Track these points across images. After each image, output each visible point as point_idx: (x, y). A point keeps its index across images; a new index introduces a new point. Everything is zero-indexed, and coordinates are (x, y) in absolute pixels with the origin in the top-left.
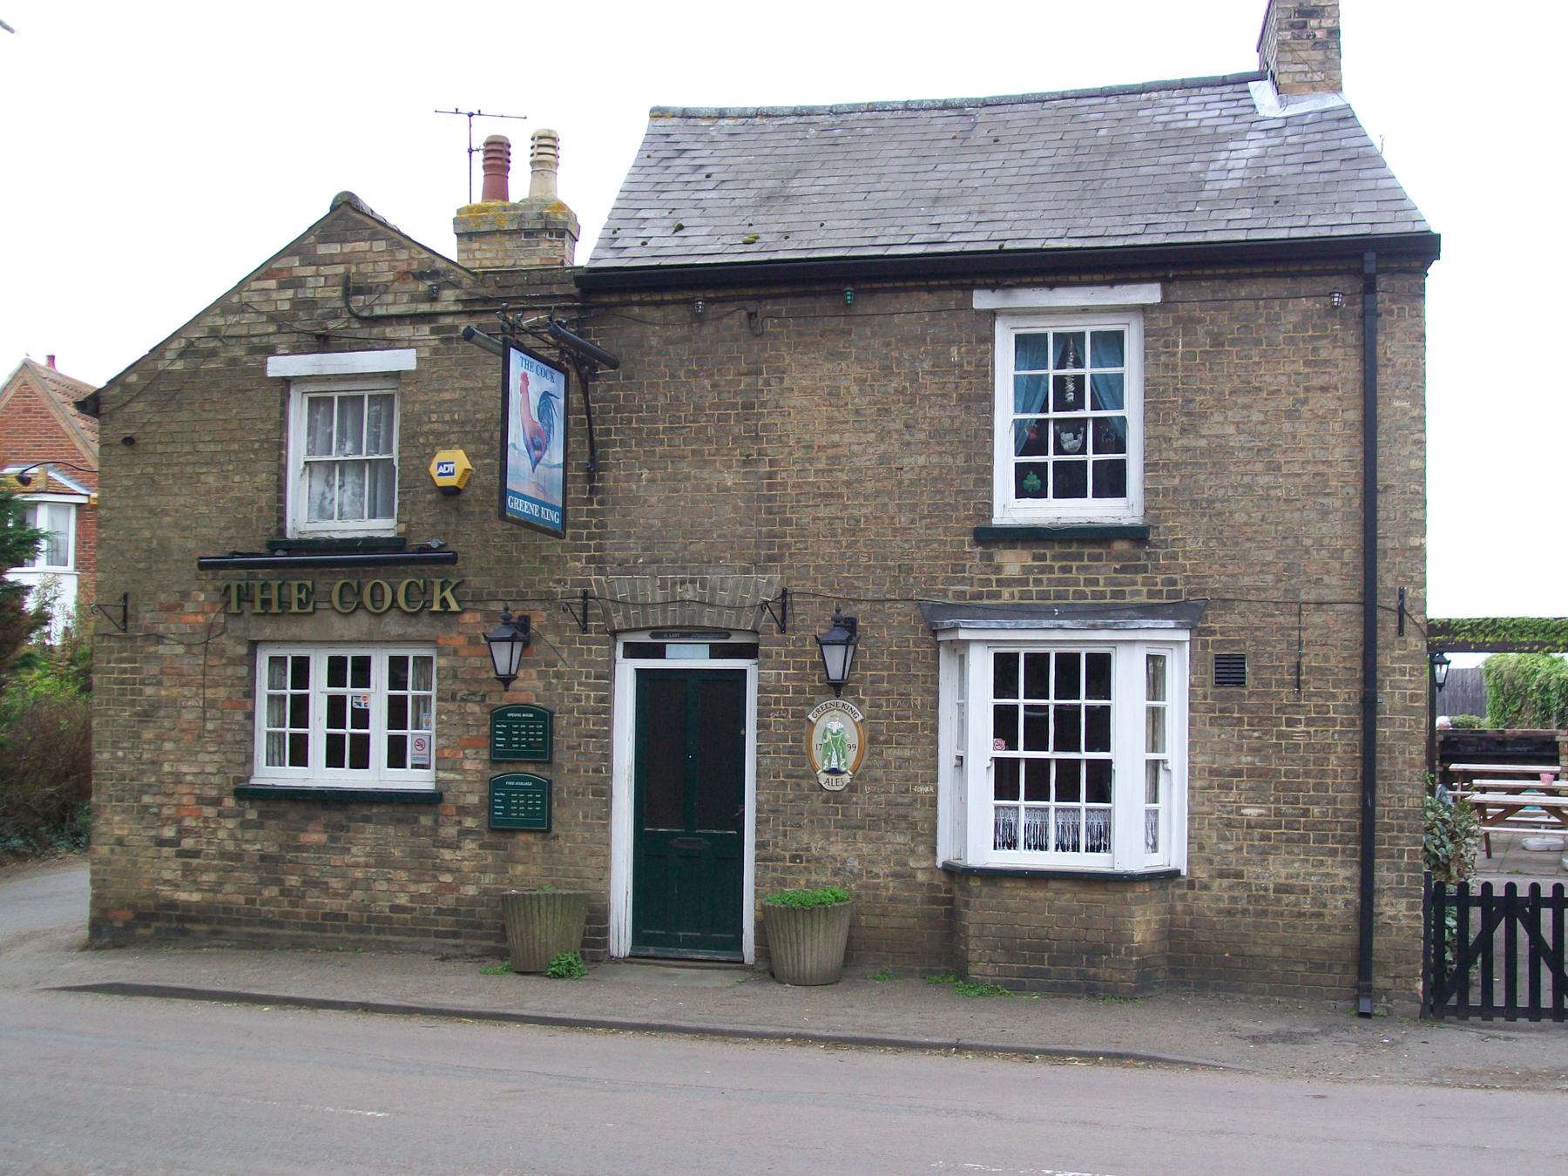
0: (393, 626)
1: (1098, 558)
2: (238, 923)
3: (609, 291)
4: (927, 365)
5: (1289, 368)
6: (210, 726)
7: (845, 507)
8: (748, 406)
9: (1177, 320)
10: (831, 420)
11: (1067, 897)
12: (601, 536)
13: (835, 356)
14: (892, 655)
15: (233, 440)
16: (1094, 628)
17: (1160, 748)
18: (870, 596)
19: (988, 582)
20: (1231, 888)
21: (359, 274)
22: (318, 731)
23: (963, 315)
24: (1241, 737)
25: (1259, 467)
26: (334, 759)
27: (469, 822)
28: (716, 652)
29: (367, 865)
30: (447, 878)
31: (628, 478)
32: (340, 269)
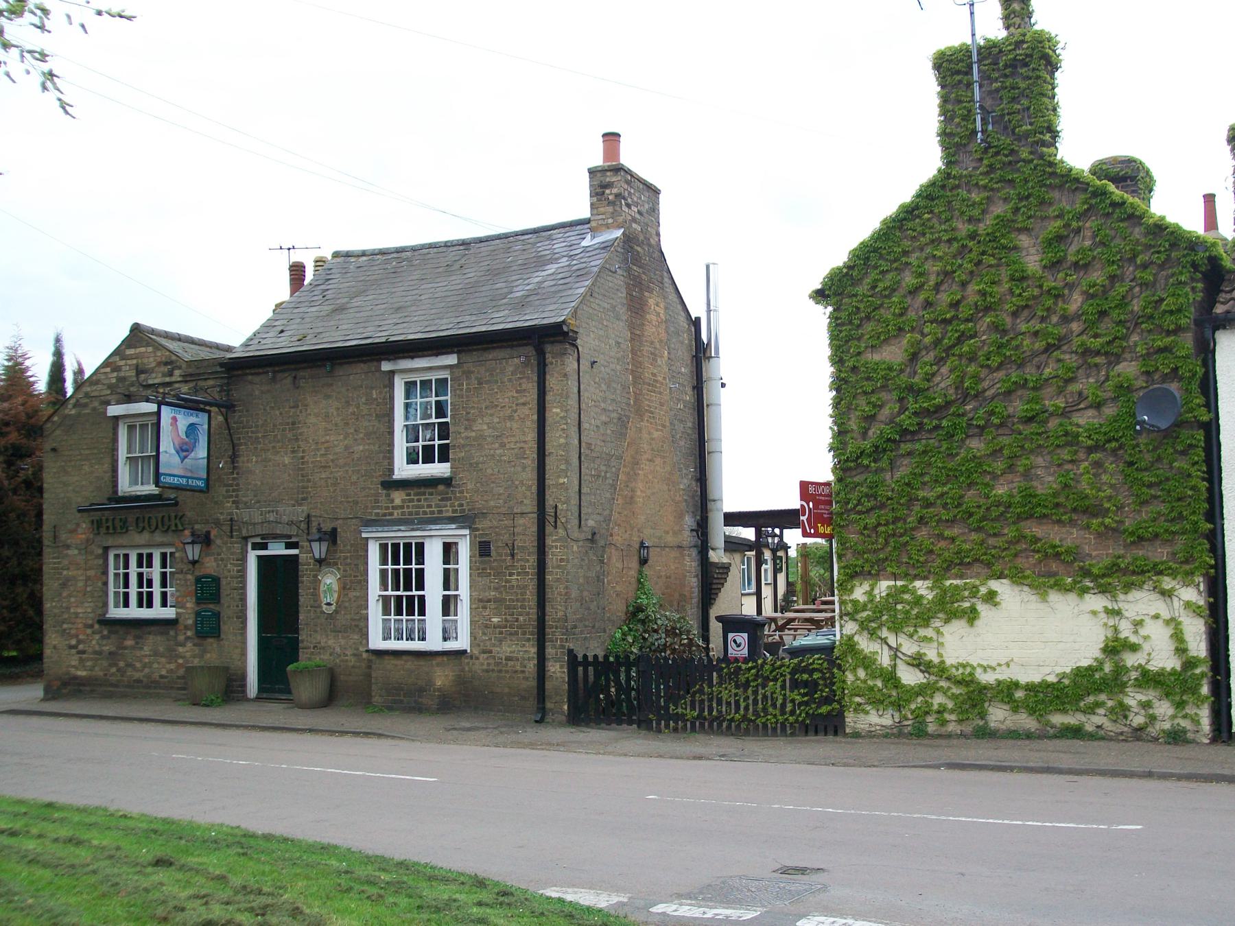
0: (158, 537)
1: (431, 494)
2: (101, 685)
3: (237, 369)
4: (363, 400)
5: (510, 394)
6: (88, 589)
7: (332, 473)
8: (293, 423)
9: (464, 372)
10: (326, 429)
11: (410, 664)
12: (238, 490)
13: (327, 397)
14: (352, 545)
15: (95, 448)
16: (413, 530)
17: (452, 585)
18: (342, 516)
19: (387, 508)
20: (487, 658)
21: (142, 363)
22: (133, 590)
23: (377, 374)
24: (491, 582)
25: (497, 445)
26: (140, 605)
27: (189, 633)
28: (289, 546)
29: (150, 656)
30: (180, 661)
31: (248, 462)
32: (135, 362)
